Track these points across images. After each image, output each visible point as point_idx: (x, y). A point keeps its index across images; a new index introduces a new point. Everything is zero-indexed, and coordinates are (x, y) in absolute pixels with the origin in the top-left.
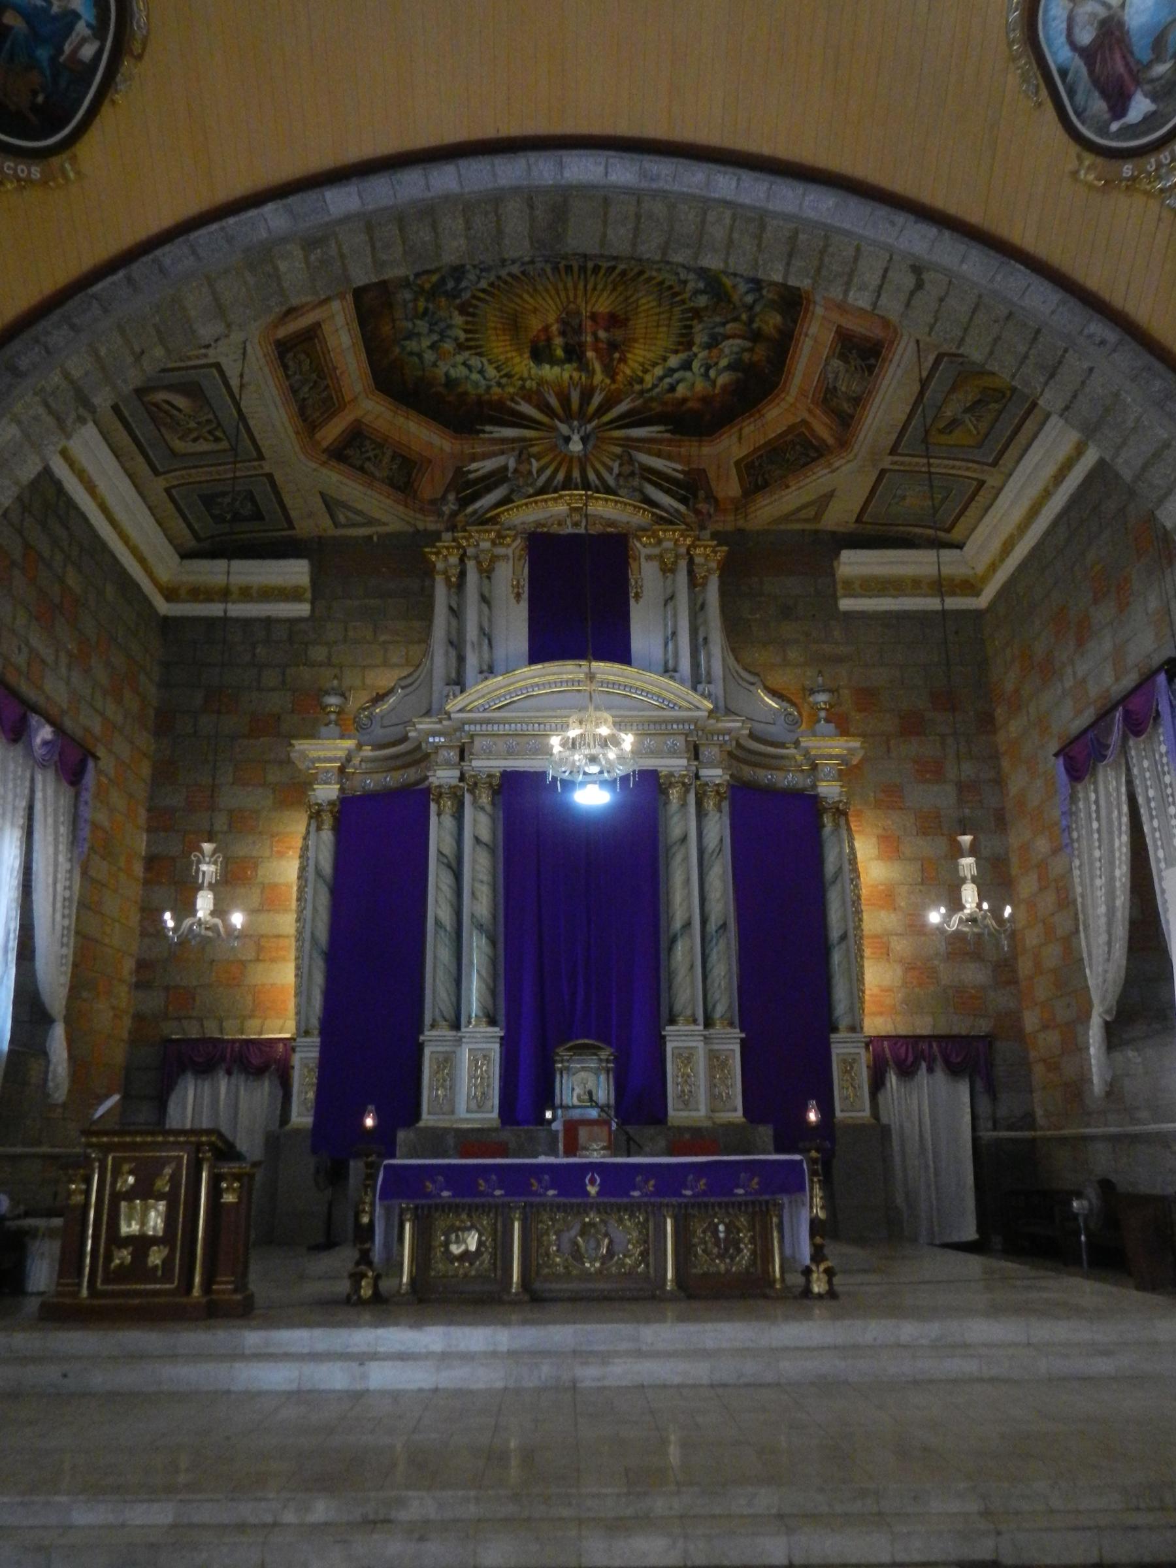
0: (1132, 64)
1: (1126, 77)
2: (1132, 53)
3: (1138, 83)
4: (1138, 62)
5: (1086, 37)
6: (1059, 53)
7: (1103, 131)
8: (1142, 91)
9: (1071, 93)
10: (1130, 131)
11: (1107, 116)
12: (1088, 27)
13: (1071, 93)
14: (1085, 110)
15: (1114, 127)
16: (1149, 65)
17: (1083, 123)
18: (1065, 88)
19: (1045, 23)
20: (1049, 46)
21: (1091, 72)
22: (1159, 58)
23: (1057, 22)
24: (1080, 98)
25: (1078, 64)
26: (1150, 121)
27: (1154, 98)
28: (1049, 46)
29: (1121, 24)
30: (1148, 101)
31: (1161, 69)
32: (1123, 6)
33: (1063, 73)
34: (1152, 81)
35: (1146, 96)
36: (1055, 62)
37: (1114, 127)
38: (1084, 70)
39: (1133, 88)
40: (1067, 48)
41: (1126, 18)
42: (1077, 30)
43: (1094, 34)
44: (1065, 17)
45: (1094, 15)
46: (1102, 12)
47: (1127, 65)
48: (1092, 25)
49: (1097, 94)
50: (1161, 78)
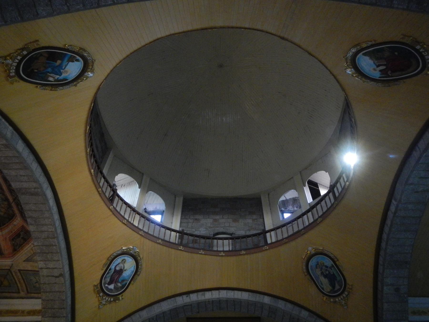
0: (118, 279)
1: (115, 280)
2: (119, 278)
3: (115, 282)
4: (118, 280)
5: (118, 268)
6: (113, 266)
7: (105, 283)
8: (115, 285)
9: (108, 273)
10: (107, 288)
11: (107, 282)
12: (119, 267)
13: (108, 273)
14: (107, 278)
15: (106, 285)
16: (119, 282)
17: (104, 280)
18: (108, 272)
19: (116, 260)
20: (113, 264)
21: (113, 274)
22: (121, 283)
23: (117, 262)
24: (108, 275)
25: (113, 271)
26: (111, 290)
27: (115, 287)
28: (113, 264)
29: (122, 272)
30: (113, 287)
31: (119, 285)
32: (125, 270)
33: (110, 269)
34: (117, 285)
35: (114, 286)
36: (111, 267)
37: (106, 285)
38: (113, 272)
39: (114, 283)
40: (114, 267)
41: (124, 273)
42: (118, 266)
43: (119, 269)
44: (119, 262)
45: (121, 267)
46: (122, 268)
47: (117, 279)
48: (120, 268)
49: (110, 278)
50: (118, 286)
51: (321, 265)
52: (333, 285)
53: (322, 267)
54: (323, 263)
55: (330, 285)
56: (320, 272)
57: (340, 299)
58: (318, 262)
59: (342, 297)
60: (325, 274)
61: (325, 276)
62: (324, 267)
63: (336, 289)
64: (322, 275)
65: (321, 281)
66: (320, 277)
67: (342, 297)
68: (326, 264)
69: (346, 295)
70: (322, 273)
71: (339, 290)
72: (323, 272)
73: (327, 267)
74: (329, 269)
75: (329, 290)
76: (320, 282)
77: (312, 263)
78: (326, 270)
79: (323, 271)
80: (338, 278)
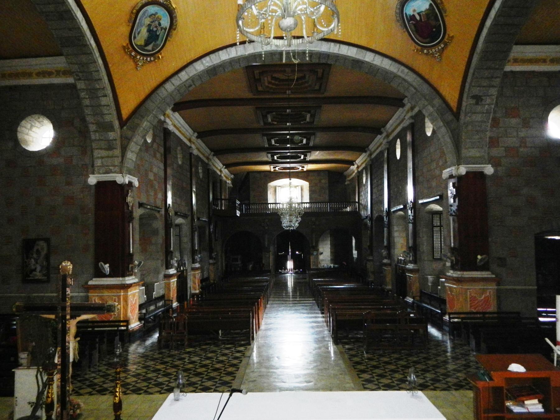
51: (157, 19)
52: (147, 43)
53: (156, 21)
54: (160, 19)
55: (145, 40)
56: (149, 23)
57: (141, 58)
58: (156, 13)
59: (145, 58)
60: (151, 29)
61: (149, 31)
62: (157, 23)
63: (146, 48)
64: (147, 28)
65: (140, 30)
66: (144, 27)
67: (145, 58)
68: (162, 22)
69: (150, 59)
70: (149, 25)
71: (149, 51)
72: (151, 25)
73: (160, 24)
74: (159, 28)
75: (139, 43)
76: (139, 30)
77: (152, 9)
78: (156, 27)
79: (153, 24)
80: (158, 42)
